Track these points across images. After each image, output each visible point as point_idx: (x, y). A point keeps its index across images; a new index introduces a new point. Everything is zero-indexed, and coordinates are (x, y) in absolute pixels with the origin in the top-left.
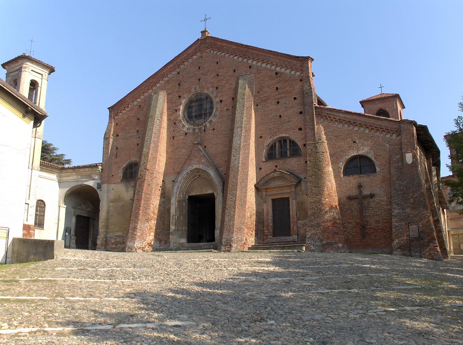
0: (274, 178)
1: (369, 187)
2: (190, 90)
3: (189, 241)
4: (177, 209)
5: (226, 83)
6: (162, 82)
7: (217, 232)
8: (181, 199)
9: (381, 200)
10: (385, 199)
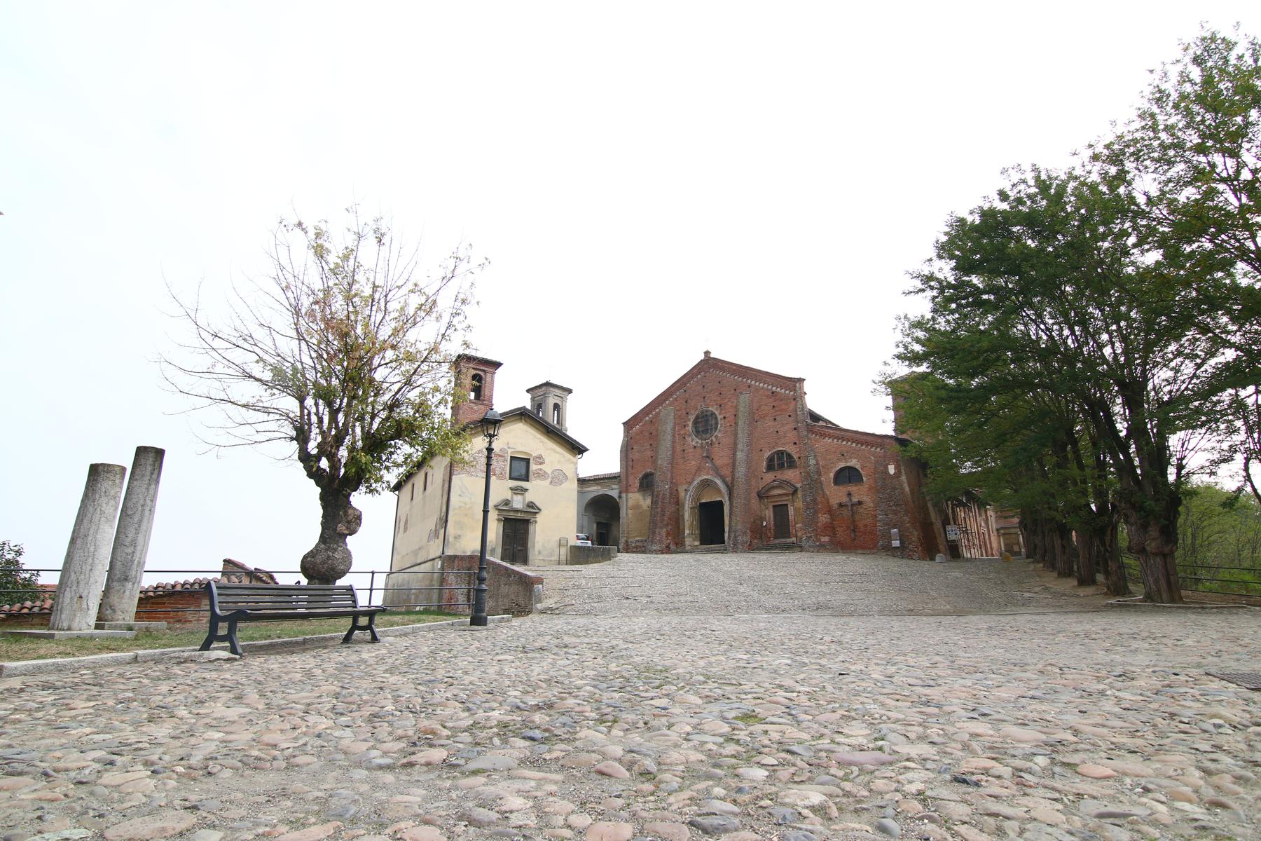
0: (774, 488)
3: (701, 544)
7: (726, 535)
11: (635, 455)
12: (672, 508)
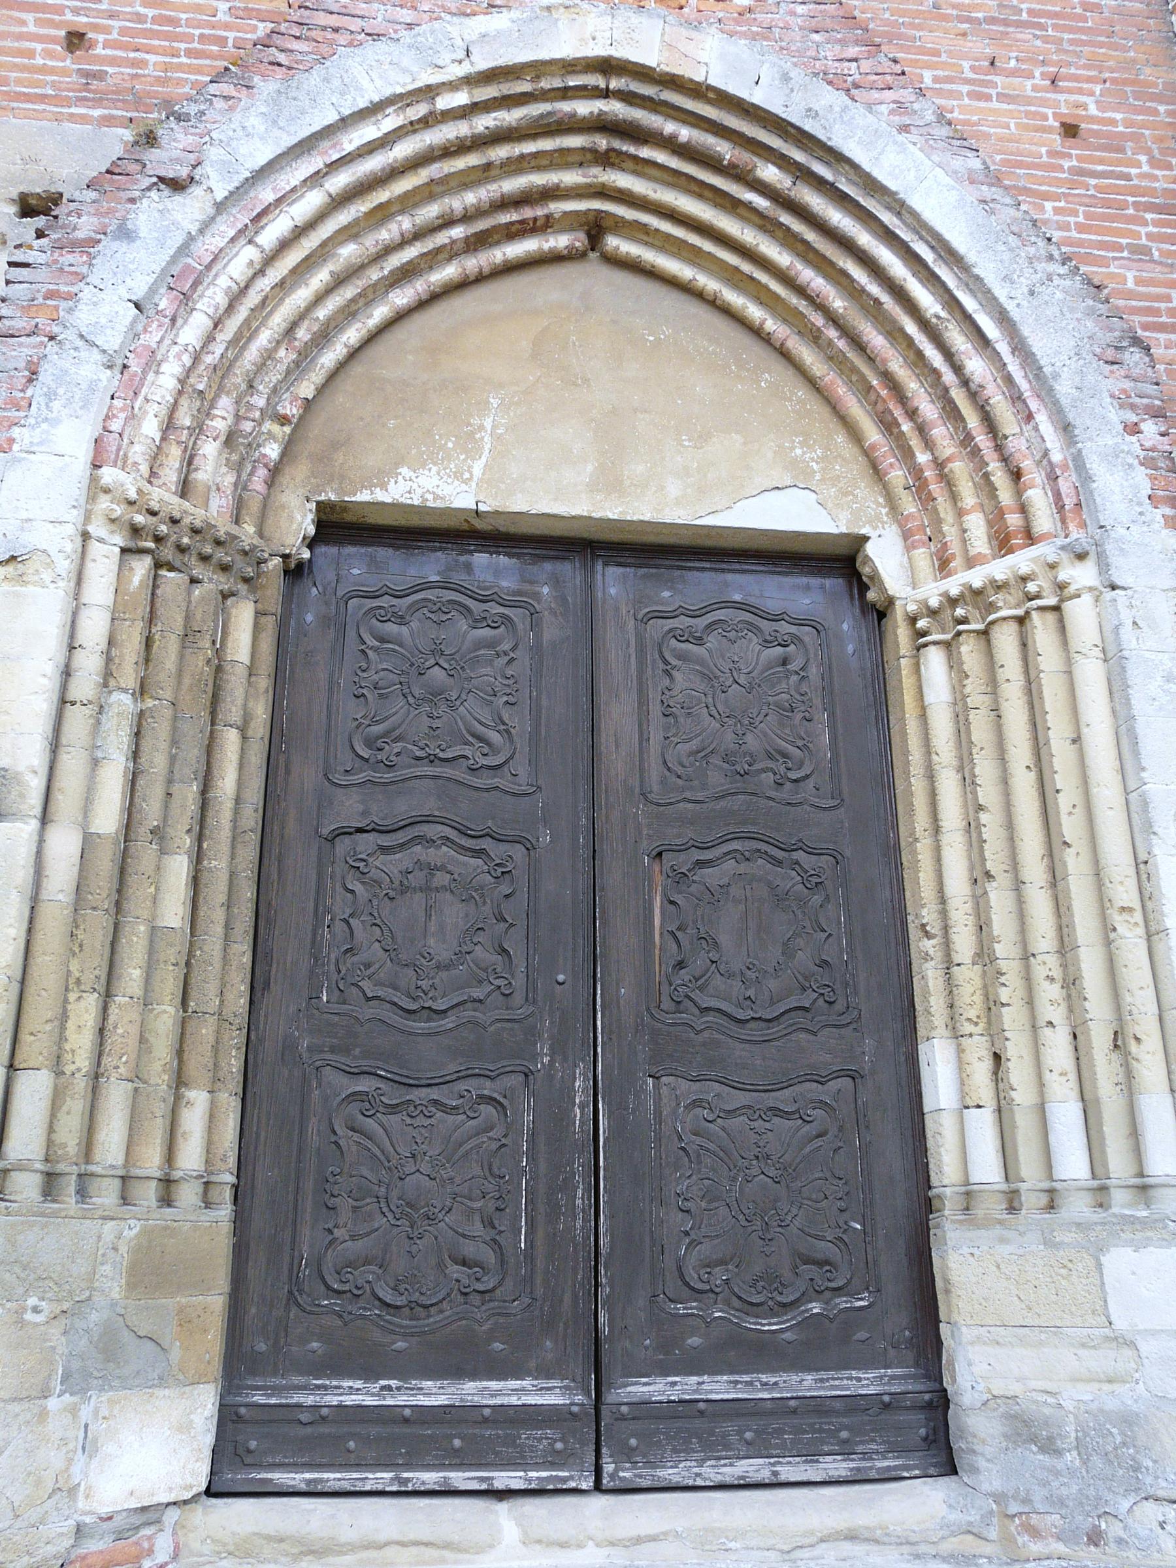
4: (108, 674)
8: (195, 514)
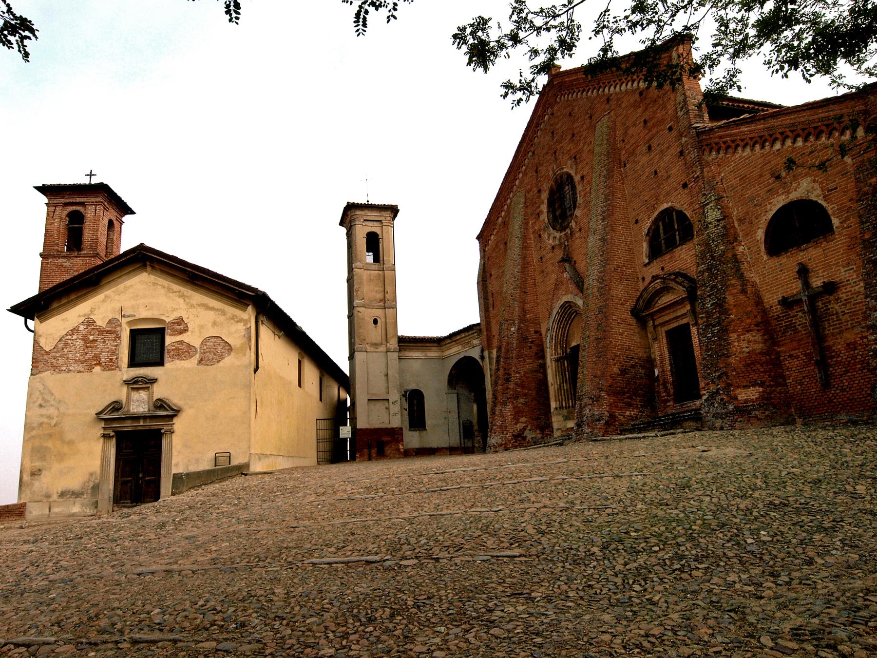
0: (659, 293)
1: (821, 269)
2: (548, 175)
5: (584, 144)
6: (521, 175)
9: (855, 294)
10: (860, 288)
11: (493, 286)
12: (529, 365)
